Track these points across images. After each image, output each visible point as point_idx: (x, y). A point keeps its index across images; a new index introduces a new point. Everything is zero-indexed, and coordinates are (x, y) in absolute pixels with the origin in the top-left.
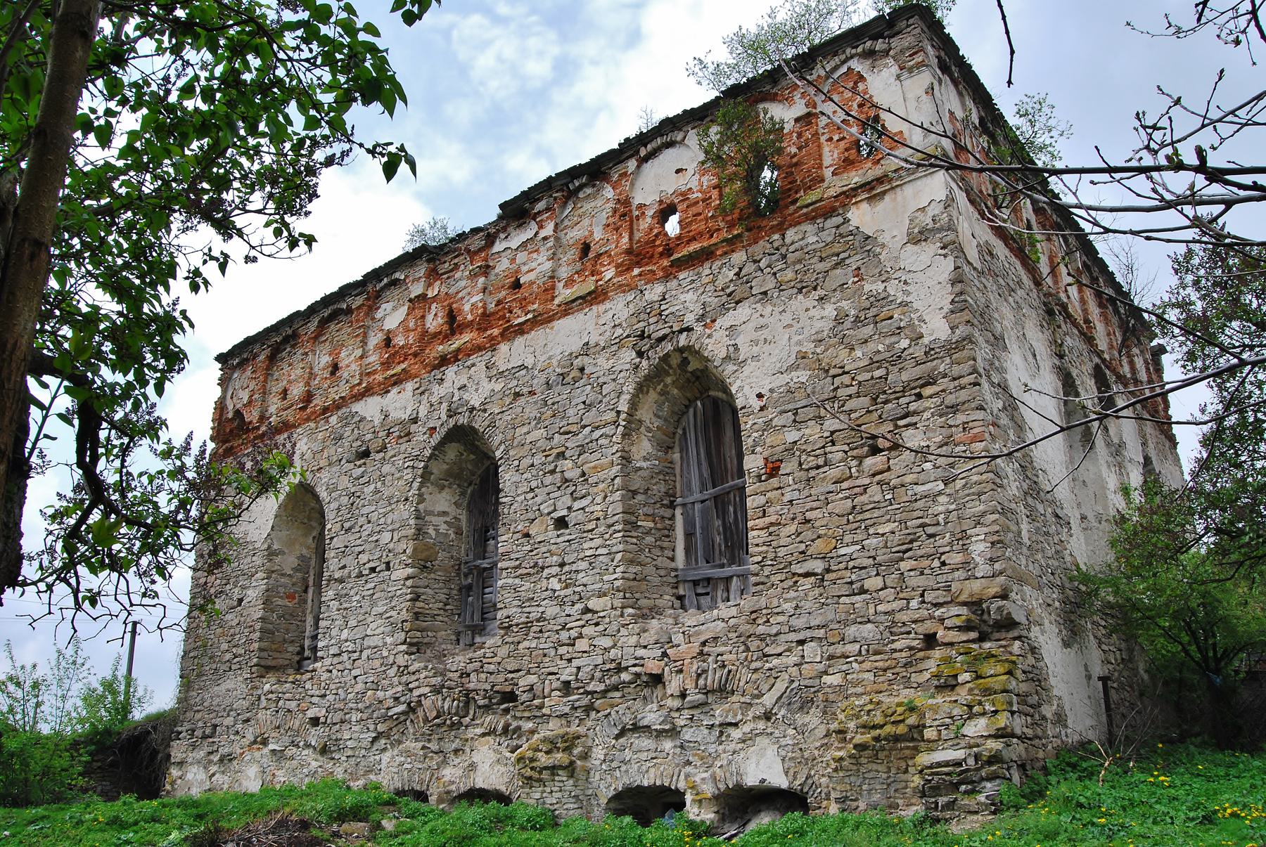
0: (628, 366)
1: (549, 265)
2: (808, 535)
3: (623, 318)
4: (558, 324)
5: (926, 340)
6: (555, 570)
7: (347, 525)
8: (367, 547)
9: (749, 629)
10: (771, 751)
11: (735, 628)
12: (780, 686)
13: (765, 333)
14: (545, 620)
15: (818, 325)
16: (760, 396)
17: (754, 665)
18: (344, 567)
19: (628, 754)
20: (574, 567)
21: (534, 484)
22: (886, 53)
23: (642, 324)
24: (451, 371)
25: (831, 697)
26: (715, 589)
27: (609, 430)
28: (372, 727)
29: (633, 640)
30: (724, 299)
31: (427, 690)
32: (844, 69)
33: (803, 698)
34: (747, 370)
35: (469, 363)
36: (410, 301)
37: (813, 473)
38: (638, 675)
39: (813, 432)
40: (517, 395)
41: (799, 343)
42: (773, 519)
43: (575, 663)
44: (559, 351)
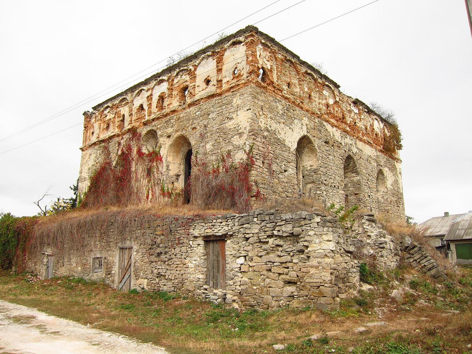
7: (326, 166)
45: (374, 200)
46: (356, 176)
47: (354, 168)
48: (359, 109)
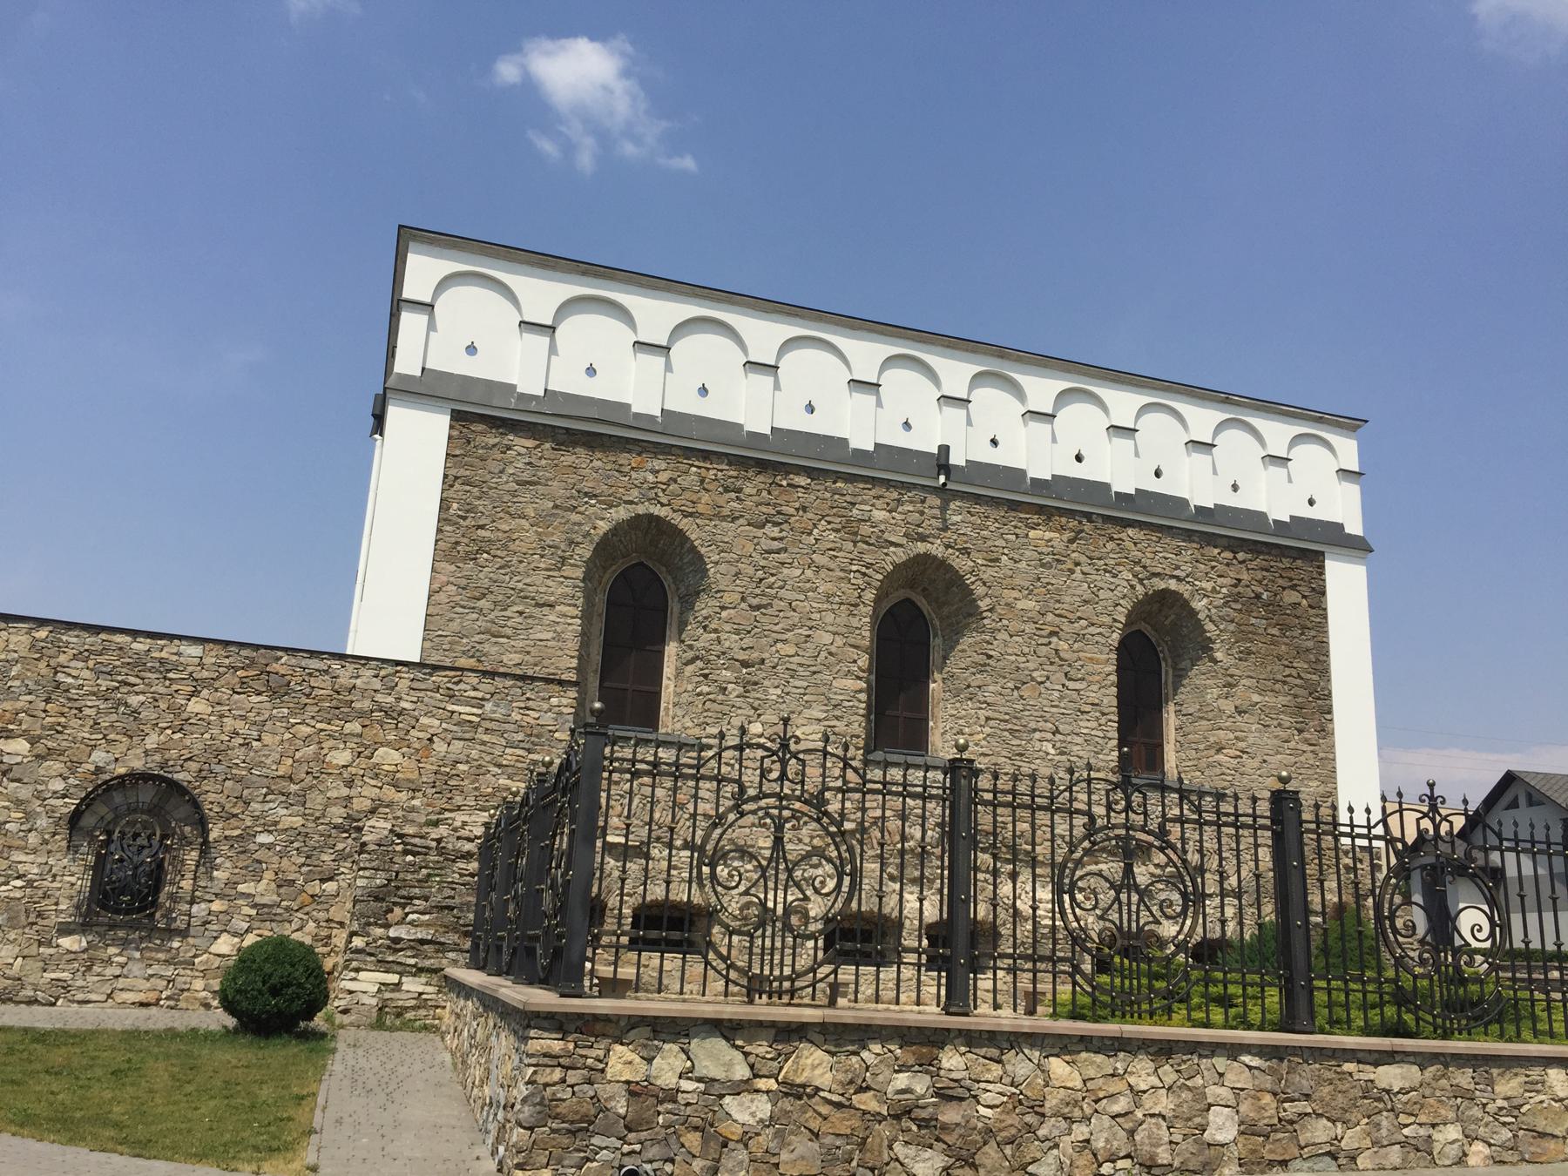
6: (1049, 736)
7: (755, 602)
20: (1069, 739)
21: (1026, 650)
28: (807, 840)
45: (1088, 708)
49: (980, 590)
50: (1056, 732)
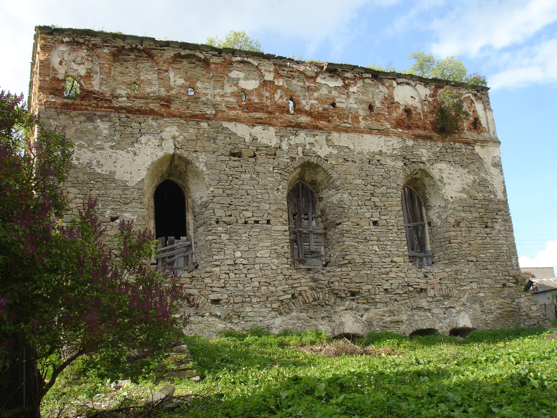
0: (401, 168)
1: (355, 106)
2: (471, 248)
3: (398, 147)
4: (366, 136)
5: (498, 198)
6: (375, 243)
7: (229, 192)
8: (251, 209)
9: (456, 276)
10: (467, 316)
11: (451, 275)
12: (467, 295)
13: (451, 176)
14: (372, 262)
15: (468, 180)
16: (451, 197)
17: (458, 288)
18: (231, 216)
19: (416, 317)
21: (360, 203)
22: (481, 99)
23: (405, 153)
24: (302, 134)
25: (482, 300)
26: (416, 260)
27: (395, 191)
29: (414, 275)
30: (436, 158)
31: (306, 288)
32: (467, 95)
33: (474, 299)
34: (447, 186)
35: (314, 133)
36: (264, 81)
37: (470, 229)
38: (415, 288)
39: (469, 216)
40: (345, 159)
41: (462, 184)
42: (460, 241)
43: (390, 282)
44: (367, 148)
46: (336, 194)
47: (329, 180)
48: (344, 79)
49: (335, 176)
50: (379, 240)
